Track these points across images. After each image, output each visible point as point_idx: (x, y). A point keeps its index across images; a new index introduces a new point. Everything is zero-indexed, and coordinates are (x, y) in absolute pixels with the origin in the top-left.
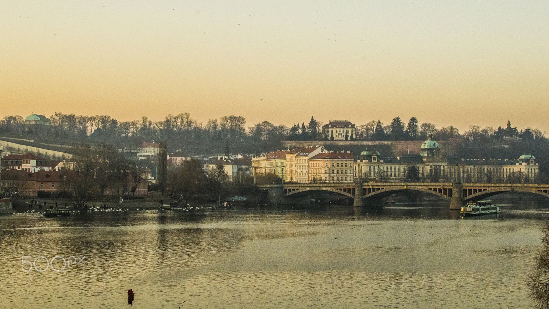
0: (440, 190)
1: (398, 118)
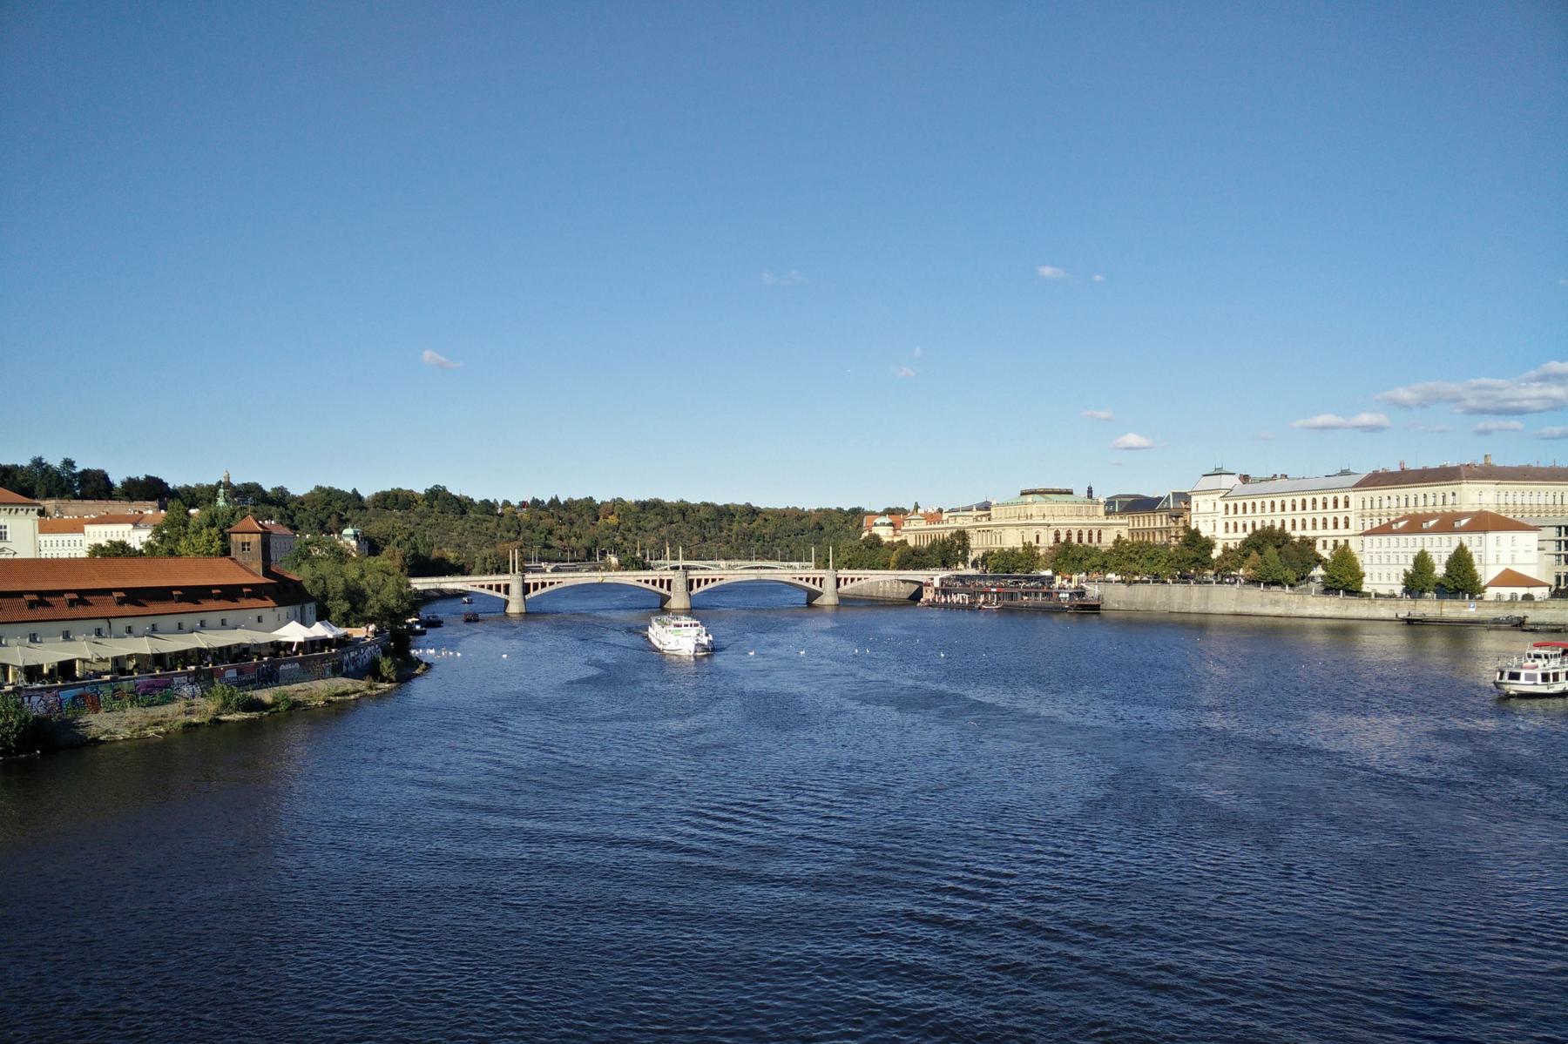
0: (654, 583)
1: (40, 459)
